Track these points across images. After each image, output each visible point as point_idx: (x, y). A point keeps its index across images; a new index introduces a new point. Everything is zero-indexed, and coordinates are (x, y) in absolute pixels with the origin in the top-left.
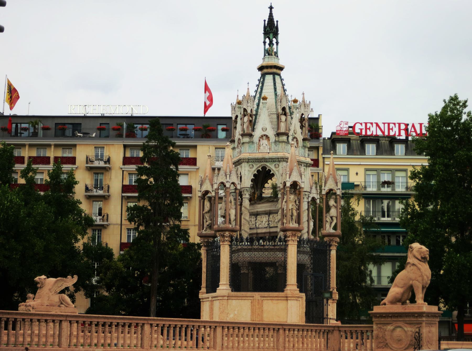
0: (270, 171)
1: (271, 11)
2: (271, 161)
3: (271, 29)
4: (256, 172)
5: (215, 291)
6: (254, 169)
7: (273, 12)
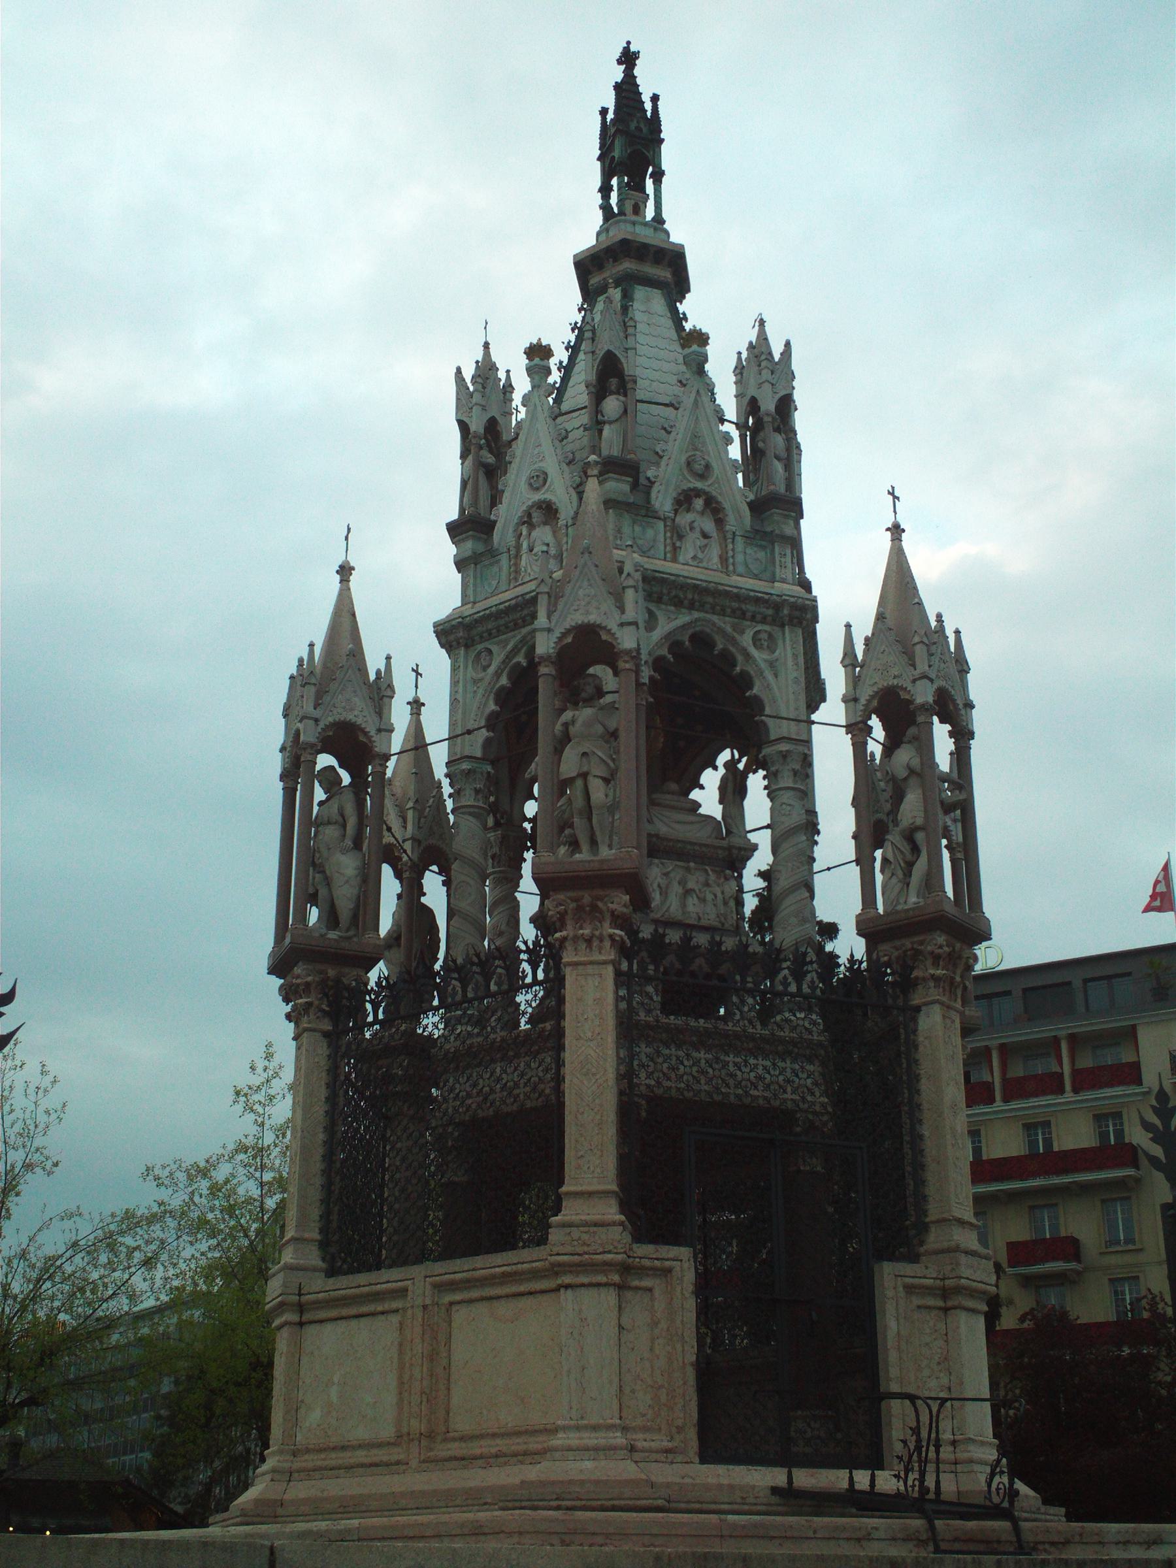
6: (657, 635)
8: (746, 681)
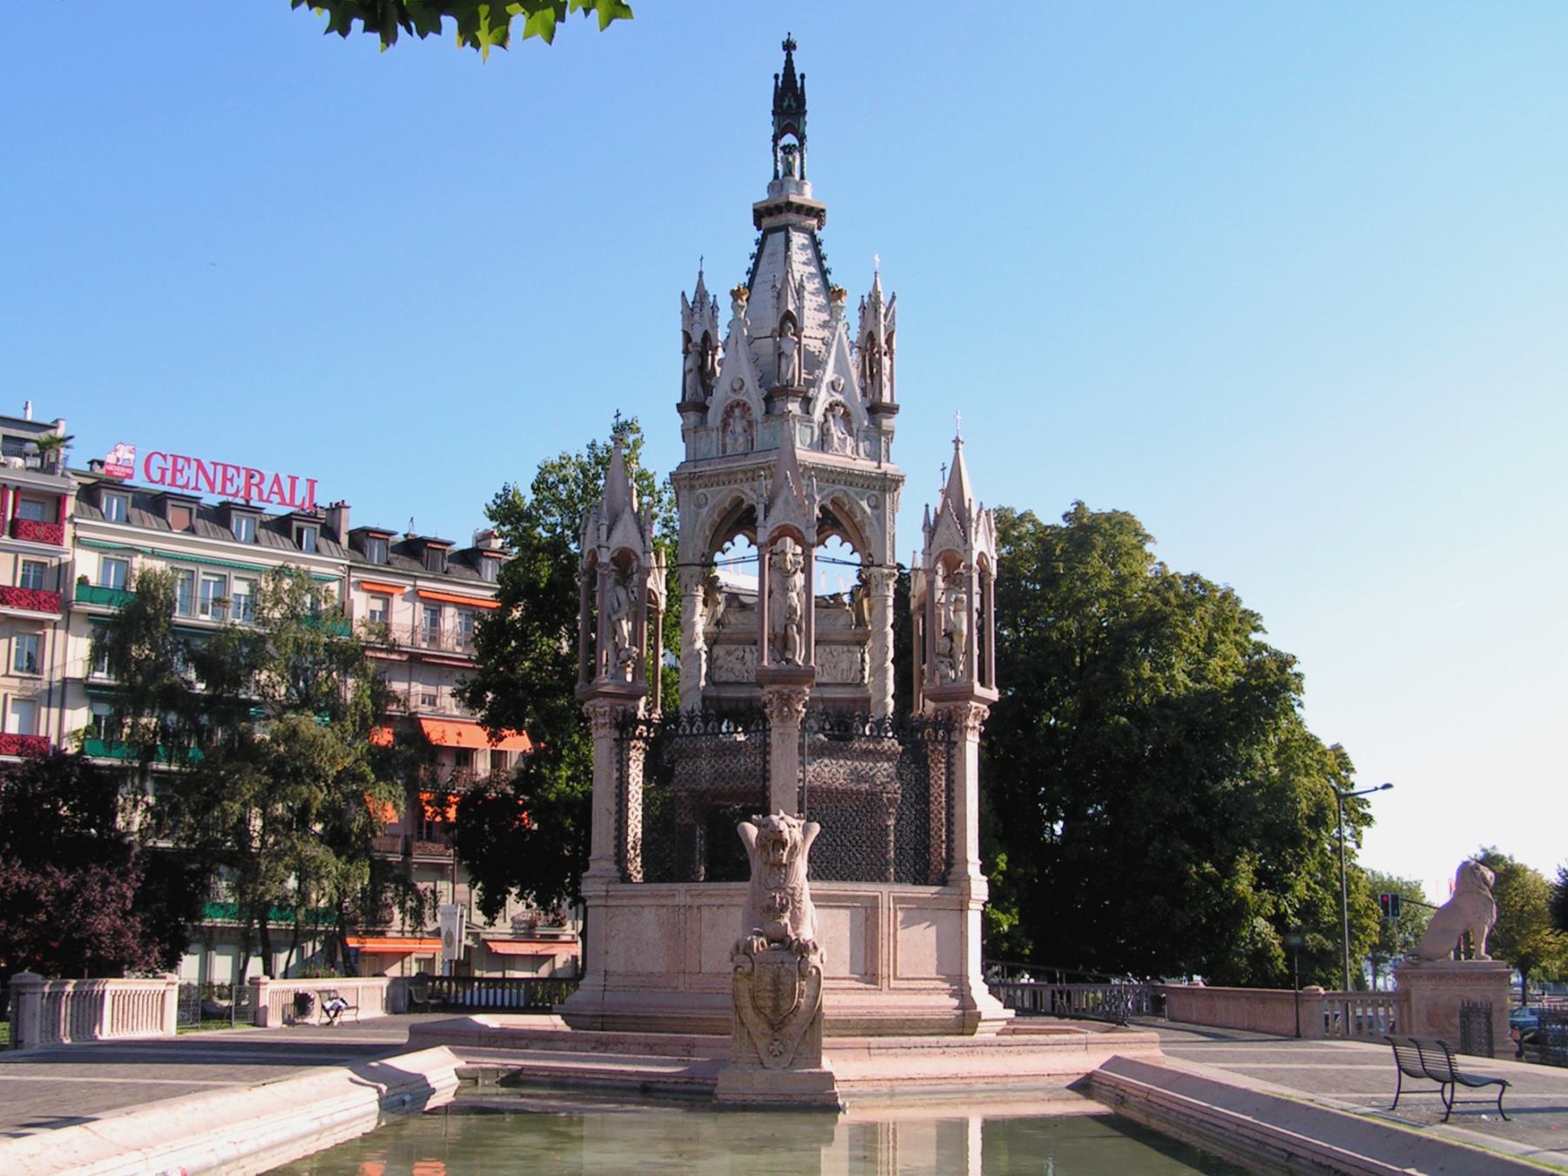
1: (789, 56)
3: (789, 103)
7: (794, 58)
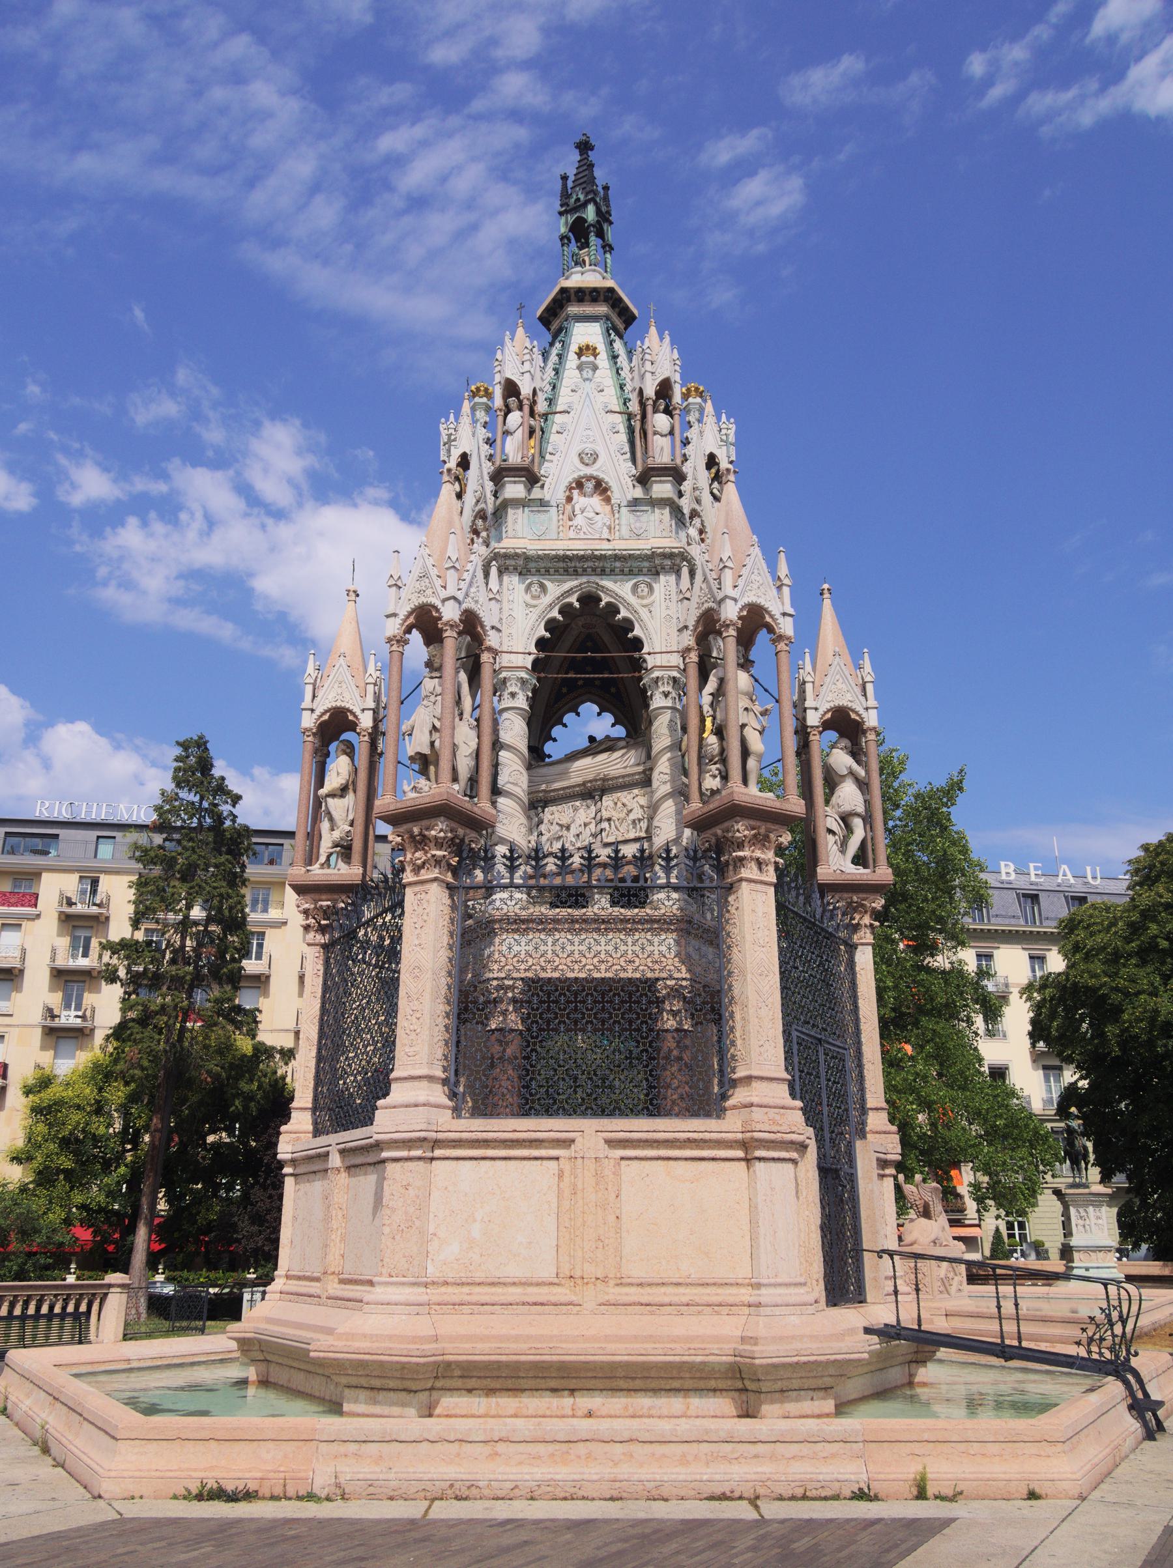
0: (613, 609)
2: (622, 572)
4: (555, 613)
5: (369, 1121)
6: (547, 600)
8: (628, 625)
